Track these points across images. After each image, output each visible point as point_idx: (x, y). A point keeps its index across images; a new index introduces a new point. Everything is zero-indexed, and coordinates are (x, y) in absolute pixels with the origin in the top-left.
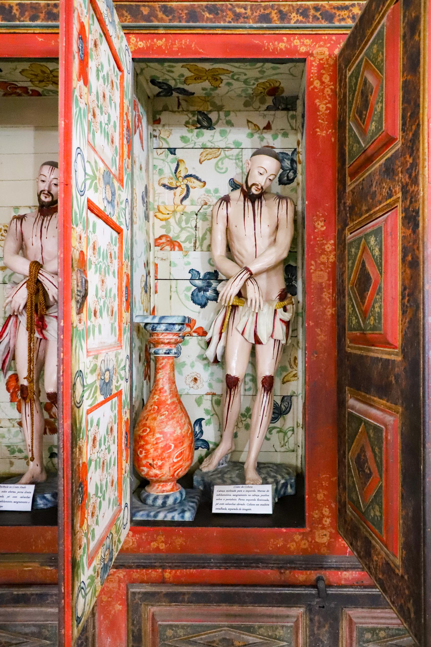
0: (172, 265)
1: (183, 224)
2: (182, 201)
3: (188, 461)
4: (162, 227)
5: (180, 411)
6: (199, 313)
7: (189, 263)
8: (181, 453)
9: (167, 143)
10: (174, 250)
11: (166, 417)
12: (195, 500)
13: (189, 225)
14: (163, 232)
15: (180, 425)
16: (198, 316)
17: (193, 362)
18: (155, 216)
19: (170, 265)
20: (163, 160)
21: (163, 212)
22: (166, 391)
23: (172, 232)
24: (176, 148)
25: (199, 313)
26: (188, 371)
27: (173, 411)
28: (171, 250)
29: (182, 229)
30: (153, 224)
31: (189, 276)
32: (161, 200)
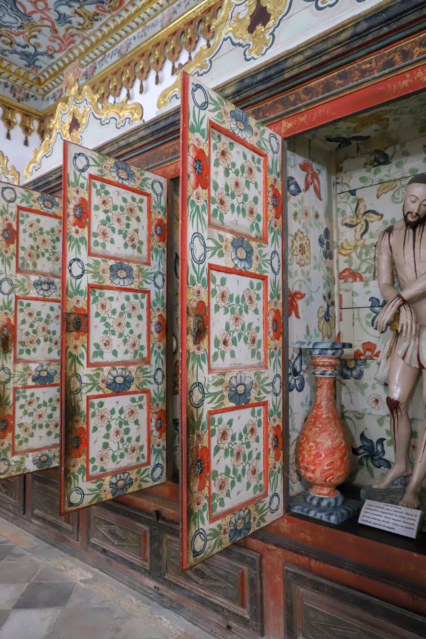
0: (354, 294)
1: (364, 257)
2: (362, 236)
3: (340, 471)
4: (346, 262)
5: (334, 425)
6: (379, 337)
7: (369, 292)
8: (332, 463)
9: (349, 186)
10: (356, 281)
11: (319, 429)
12: (349, 509)
13: (369, 257)
14: (346, 266)
15: (332, 437)
16: (379, 341)
17: (374, 384)
18: (340, 253)
19: (353, 295)
20: (345, 202)
21: (347, 248)
22: (322, 407)
23: (354, 266)
24: (355, 190)
25: (379, 337)
26: (369, 391)
27: (326, 425)
28: (353, 281)
29: (363, 261)
30: (338, 260)
31: (369, 304)
32: (344, 238)
